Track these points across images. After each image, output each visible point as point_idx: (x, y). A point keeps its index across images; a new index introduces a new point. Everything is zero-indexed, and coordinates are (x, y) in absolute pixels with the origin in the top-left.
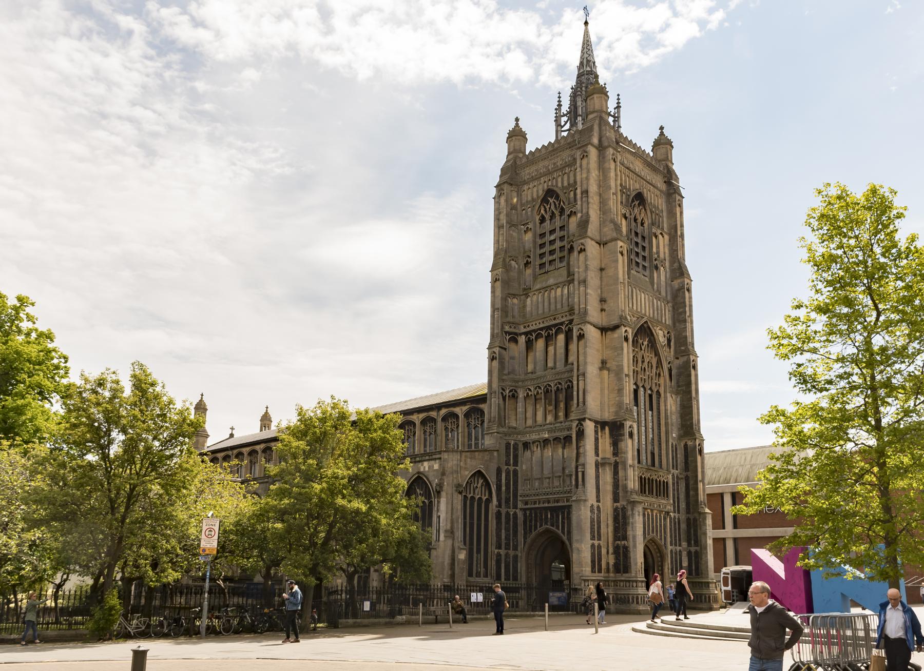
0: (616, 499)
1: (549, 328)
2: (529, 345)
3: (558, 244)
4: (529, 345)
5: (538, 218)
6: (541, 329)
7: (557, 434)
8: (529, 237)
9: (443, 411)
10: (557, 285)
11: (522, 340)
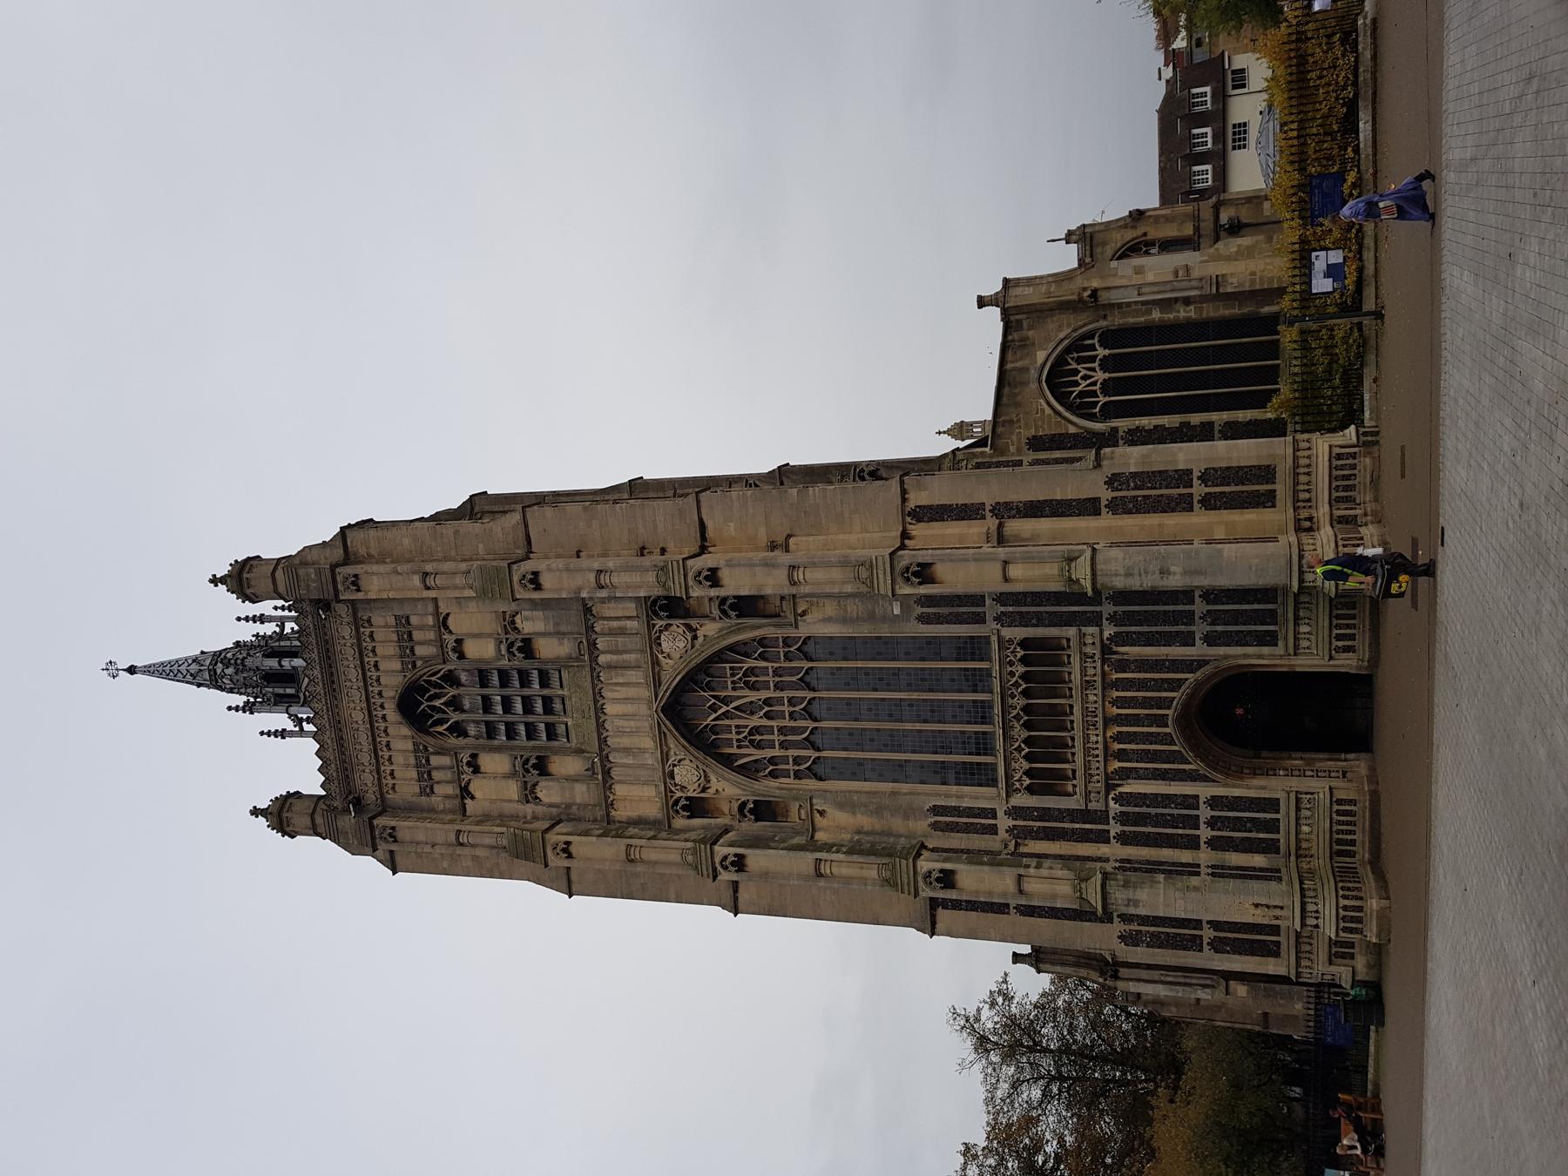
0: (1090, 507)
5: (453, 741)
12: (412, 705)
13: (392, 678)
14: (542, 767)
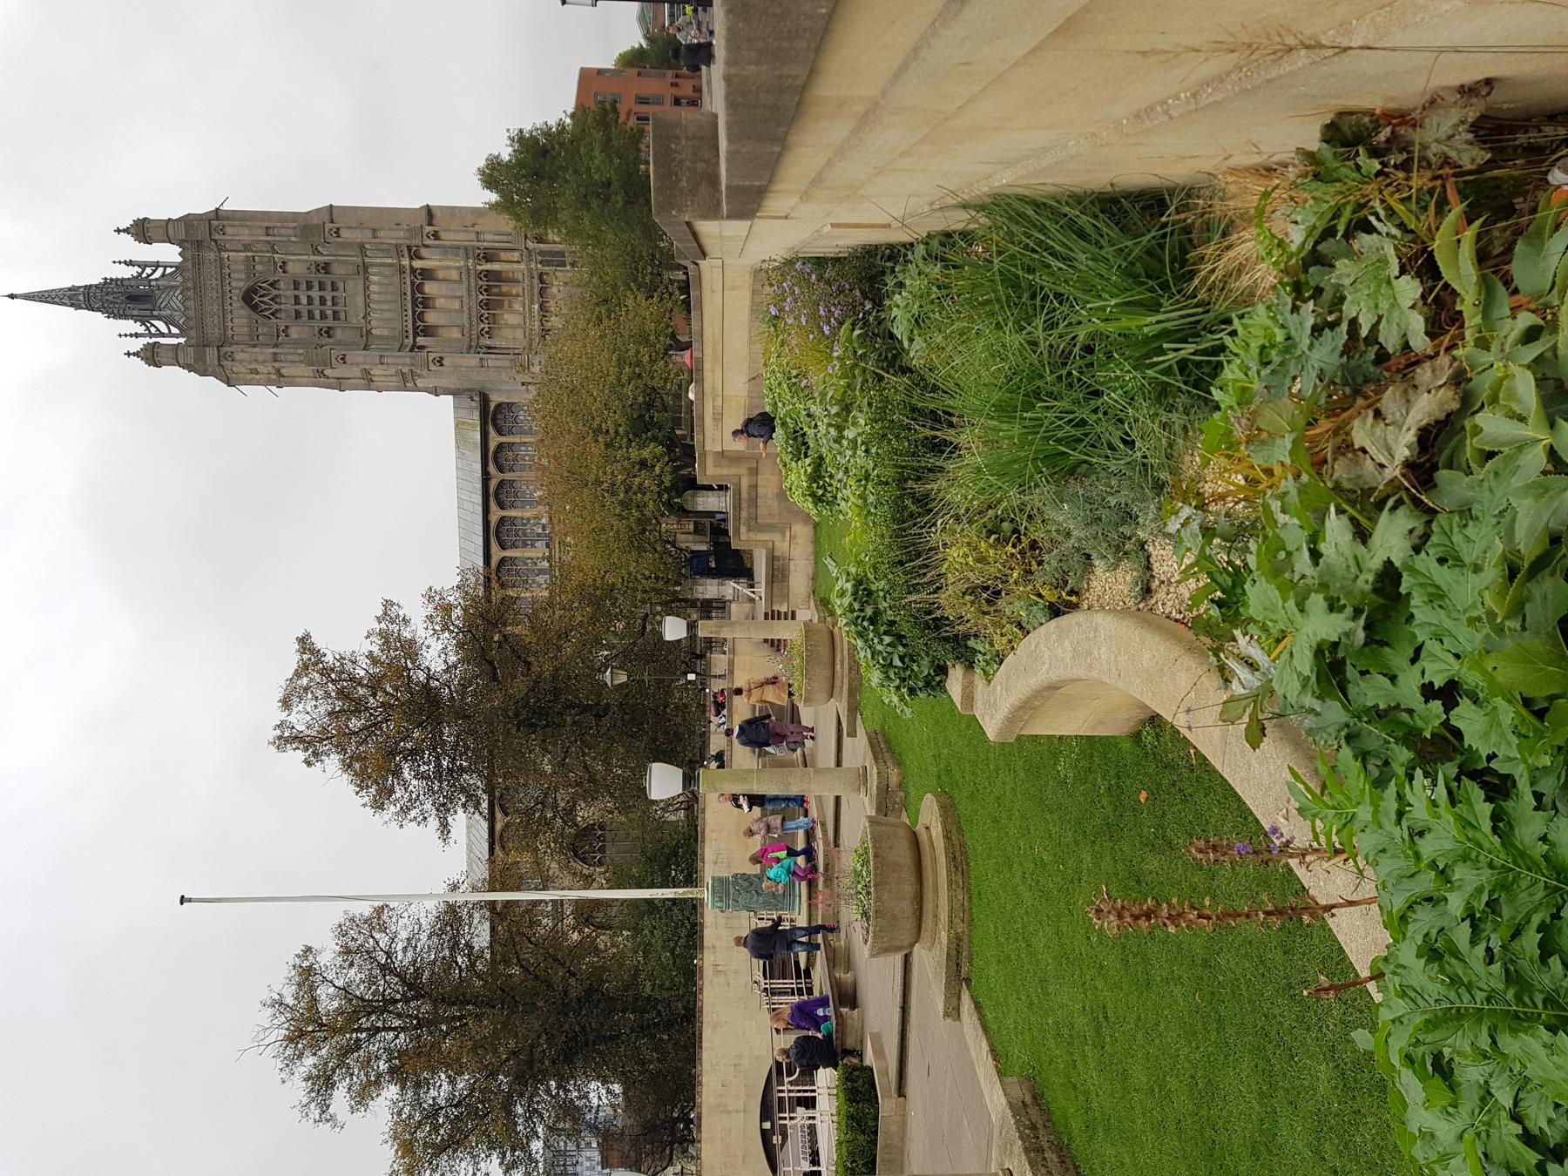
1: (414, 301)
2: (428, 331)
3: (315, 294)
4: (428, 331)
6: (414, 312)
7: (536, 291)
8: (295, 332)
9: (492, 469)
10: (366, 288)
11: (421, 340)
12: (248, 297)
13: (239, 283)
14: (329, 332)
